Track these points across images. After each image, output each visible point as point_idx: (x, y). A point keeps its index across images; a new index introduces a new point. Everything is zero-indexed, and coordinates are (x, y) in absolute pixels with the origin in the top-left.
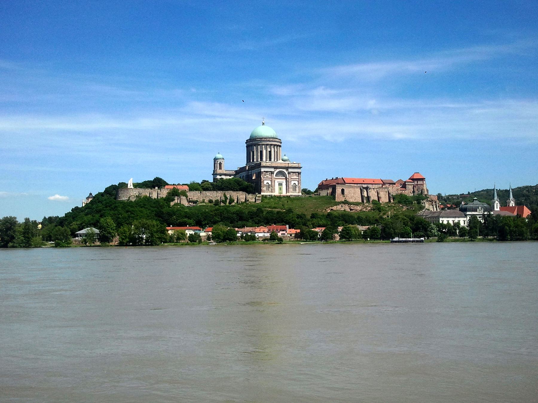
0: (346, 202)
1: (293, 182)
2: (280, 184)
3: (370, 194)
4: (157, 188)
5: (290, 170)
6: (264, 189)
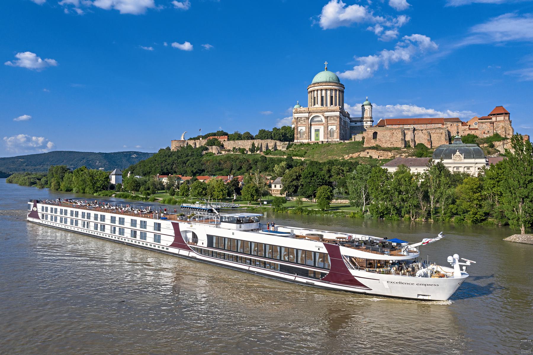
2: (317, 131)
5: (327, 114)
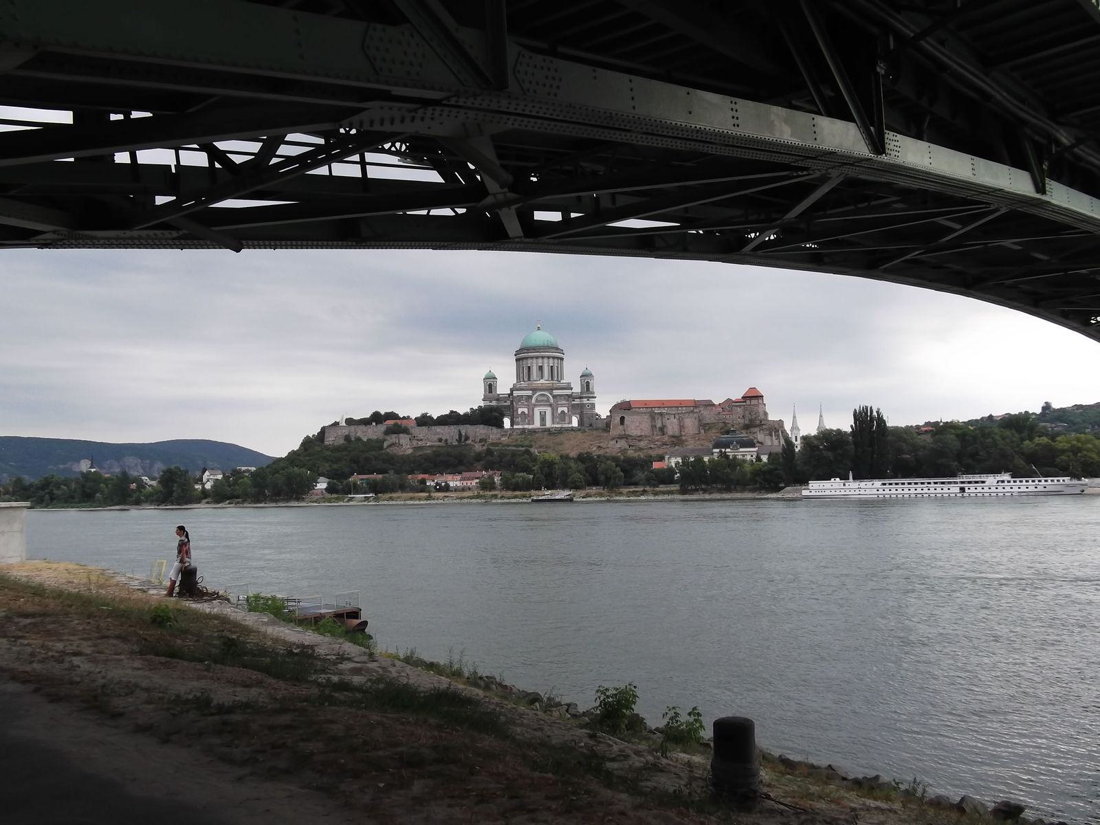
0: (625, 437)
1: (560, 410)
3: (668, 423)
4: (374, 424)
5: (556, 392)
6: (517, 420)
